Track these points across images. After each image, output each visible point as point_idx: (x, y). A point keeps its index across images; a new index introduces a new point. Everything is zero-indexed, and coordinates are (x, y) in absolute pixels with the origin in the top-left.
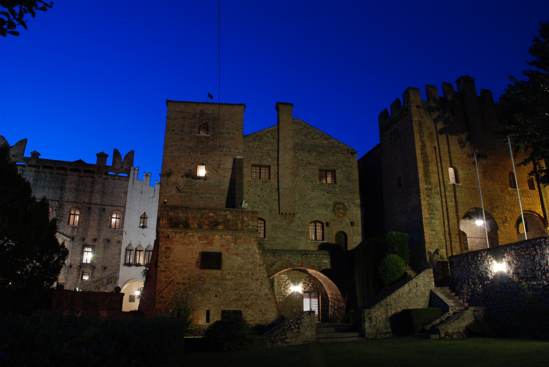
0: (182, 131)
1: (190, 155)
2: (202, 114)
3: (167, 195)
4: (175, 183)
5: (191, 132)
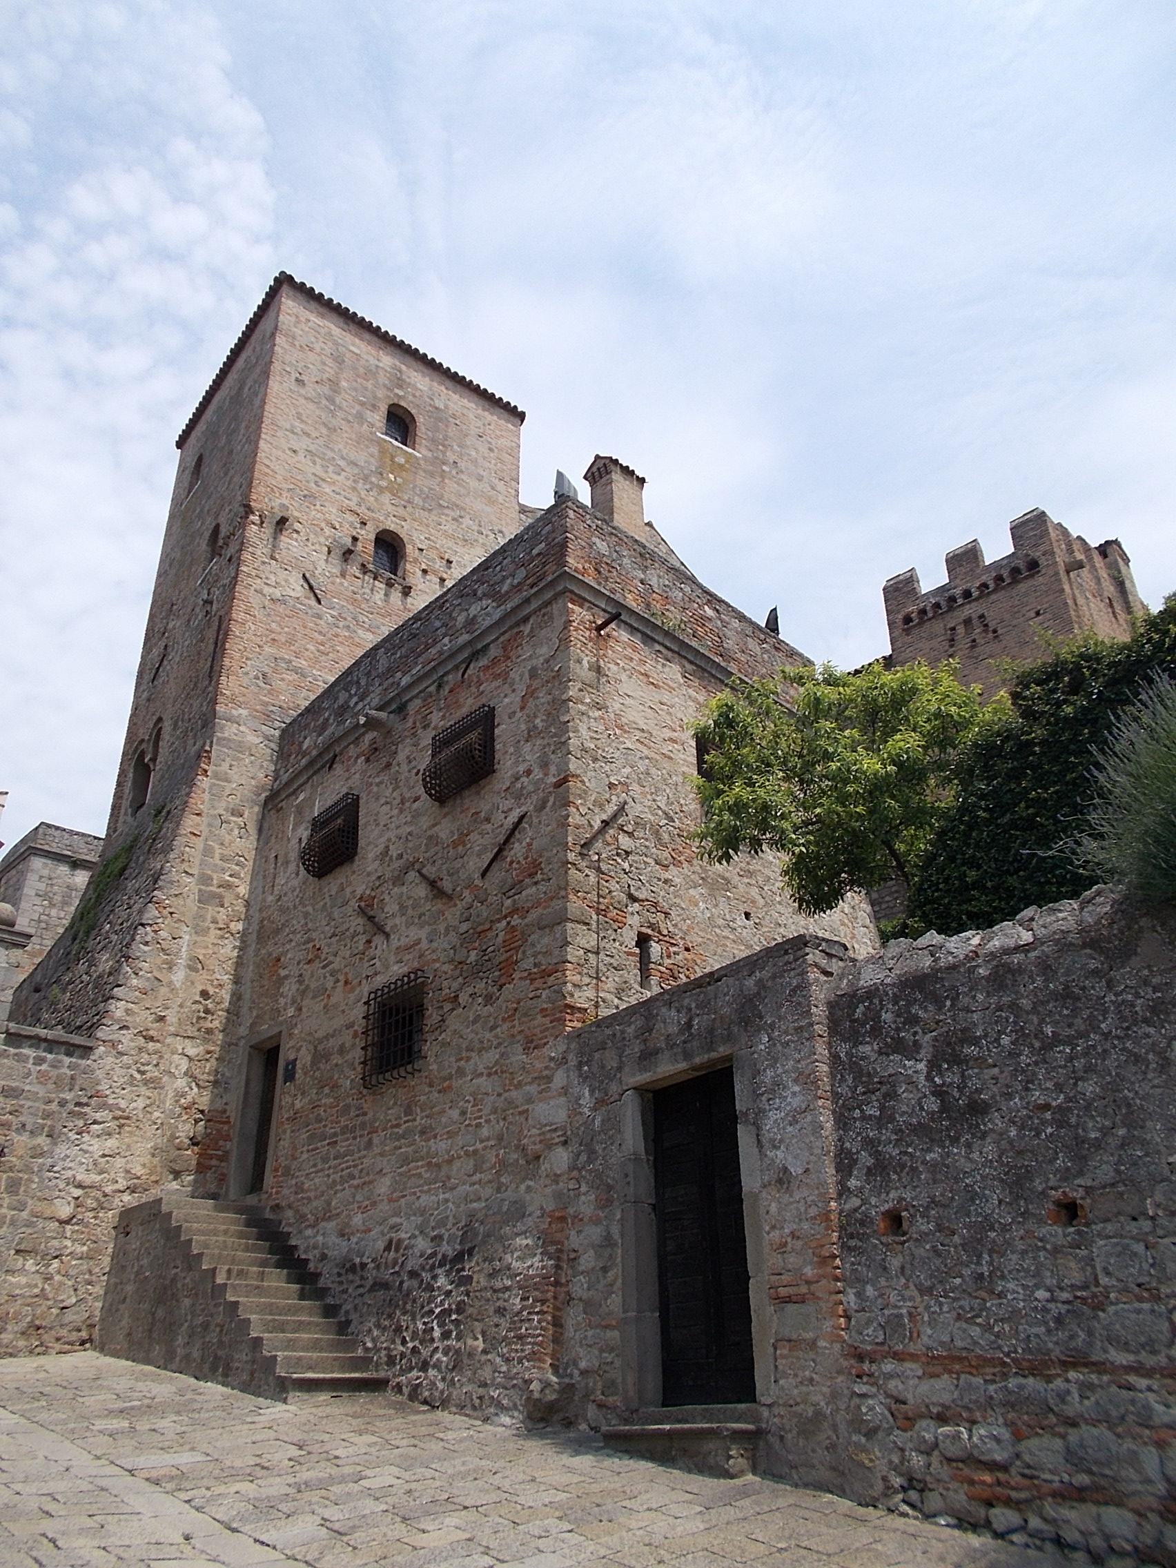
0: (331, 400)
2: (400, 382)
3: (267, 590)
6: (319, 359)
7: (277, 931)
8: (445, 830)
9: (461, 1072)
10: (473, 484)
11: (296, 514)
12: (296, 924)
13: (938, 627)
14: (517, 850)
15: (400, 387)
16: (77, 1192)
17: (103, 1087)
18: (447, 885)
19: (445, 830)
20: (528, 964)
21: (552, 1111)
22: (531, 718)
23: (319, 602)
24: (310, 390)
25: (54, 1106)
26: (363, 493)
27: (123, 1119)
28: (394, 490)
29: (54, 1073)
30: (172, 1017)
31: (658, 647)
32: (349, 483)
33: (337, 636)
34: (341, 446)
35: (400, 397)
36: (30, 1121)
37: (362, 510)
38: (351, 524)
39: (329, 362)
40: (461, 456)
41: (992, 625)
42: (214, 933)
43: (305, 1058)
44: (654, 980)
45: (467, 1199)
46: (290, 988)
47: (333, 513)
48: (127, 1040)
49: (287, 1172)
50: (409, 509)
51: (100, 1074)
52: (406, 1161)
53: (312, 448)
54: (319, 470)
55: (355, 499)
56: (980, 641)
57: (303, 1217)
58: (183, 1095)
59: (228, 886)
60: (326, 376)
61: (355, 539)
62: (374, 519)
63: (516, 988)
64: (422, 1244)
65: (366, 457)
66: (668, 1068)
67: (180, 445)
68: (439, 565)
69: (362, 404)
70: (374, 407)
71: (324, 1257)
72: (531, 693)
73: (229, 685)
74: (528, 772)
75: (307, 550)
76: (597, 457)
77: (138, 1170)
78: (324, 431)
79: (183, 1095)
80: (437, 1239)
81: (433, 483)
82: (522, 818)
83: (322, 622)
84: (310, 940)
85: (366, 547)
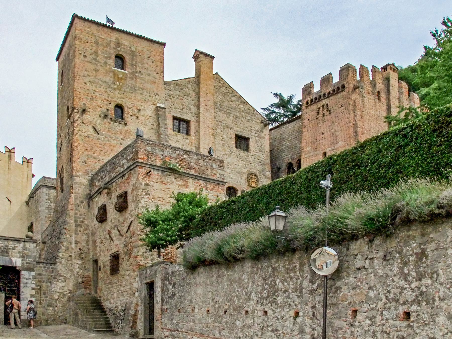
1: (106, 92)
2: (118, 44)
3: (83, 134)
4: (90, 122)
5: (106, 63)
6: (90, 45)
7: (95, 234)
8: (121, 219)
9: (125, 275)
12: (98, 233)
13: (314, 107)
14: (131, 228)
15: (119, 47)
16: (58, 294)
17: (60, 272)
18: (121, 232)
19: (121, 219)
20: (133, 254)
21: (136, 285)
22: (133, 197)
23: (98, 134)
25: (50, 277)
26: (109, 92)
27: (65, 279)
28: (120, 88)
29: (48, 270)
30: (73, 256)
31: (166, 173)
32: (104, 90)
33: (105, 144)
35: (119, 51)
36: (45, 280)
37: (110, 99)
38: (106, 105)
39: (94, 45)
42: (80, 234)
43: (102, 266)
44: (162, 257)
45: (127, 299)
46: (98, 249)
47: (100, 102)
48: (63, 261)
49: (101, 290)
51: (58, 269)
52: (118, 291)
54: (94, 88)
55: (107, 95)
56: (326, 114)
57: (104, 299)
59: (82, 222)
60: (93, 51)
62: (113, 101)
63: (131, 260)
64: (120, 307)
65: (109, 79)
66: (148, 281)
67: (57, 59)
69: (106, 58)
70: (110, 58)
71: (107, 308)
72: (133, 191)
74: (133, 210)
77: (70, 289)
80: (122, 306)
81: (132, 82)
82: (132, 221)
83: (100, 141)
84: (100, 238)
85: (112, 113)
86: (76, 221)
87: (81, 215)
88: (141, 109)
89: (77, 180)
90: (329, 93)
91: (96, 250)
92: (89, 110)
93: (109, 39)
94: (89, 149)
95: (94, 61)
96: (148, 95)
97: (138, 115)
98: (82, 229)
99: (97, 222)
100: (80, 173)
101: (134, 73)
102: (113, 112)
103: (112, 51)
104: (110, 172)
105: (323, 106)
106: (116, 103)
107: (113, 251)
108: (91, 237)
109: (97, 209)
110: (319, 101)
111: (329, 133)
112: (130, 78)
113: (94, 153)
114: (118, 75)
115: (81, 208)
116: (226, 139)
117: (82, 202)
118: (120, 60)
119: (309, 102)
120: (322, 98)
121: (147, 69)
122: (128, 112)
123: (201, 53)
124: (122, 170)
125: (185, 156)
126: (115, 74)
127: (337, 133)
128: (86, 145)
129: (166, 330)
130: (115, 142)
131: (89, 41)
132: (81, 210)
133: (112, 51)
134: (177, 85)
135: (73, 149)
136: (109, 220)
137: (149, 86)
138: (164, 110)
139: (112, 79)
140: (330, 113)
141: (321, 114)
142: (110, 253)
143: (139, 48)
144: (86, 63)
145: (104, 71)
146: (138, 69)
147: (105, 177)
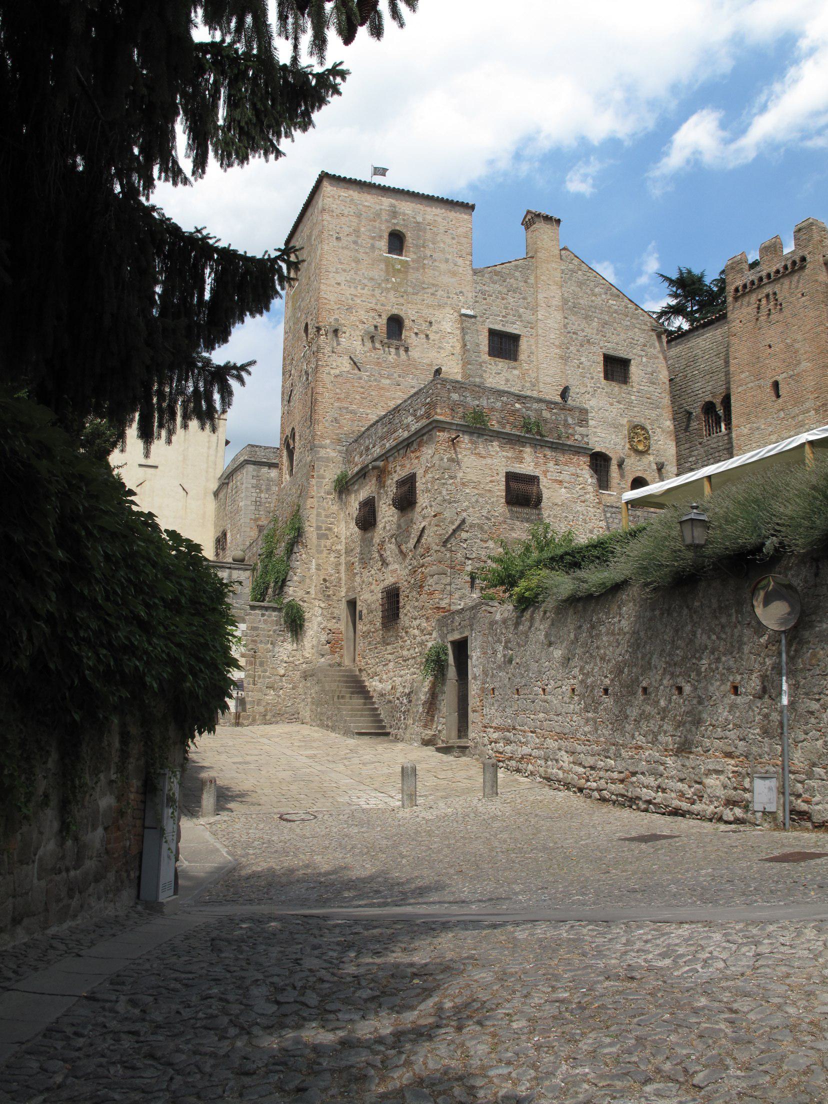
0: (355, 242)
1: (373, 296)
2: (394, 214)
3: (332, 372)
5: (373, 247)
10: (443, 266)
11: (343, 322)
15: (395, 217)
24: (345, 241)
29: (270, 619)
30: (312, 591)
34: (364, 271)
37: (378, 307)
38: (373, 318)
40: (434, 250)
41: (780, 300)
47: (363, 315)
50: (405, 297)
53: (348, 278)
58: (322, 623)
61: (376, 327)
65: (378, 272)
68: (424, 326)
69: (373, 238)
70: (381, 237)
73: (319, 429)
75: (352, 341)
76: (528, 212)
78: (353, 265)
79: (322, 623)
86: (319, 528)
87: (327, 516)
88: (433, 321)
89: (322, 453)
90: (778, 272)
91: (353, 581)
92: (344, 329)
93: (378, 207)
94: (342, 396)
95: (353, 246)
96: (445, 295)
97: (428, 332)
98: (328, 543)
99: (357, 529)
100: (328, 441)
101: (419, 260)
102: (385, 329)
103: (383, 227)
104: (382, 438)
105: (767, 296)
106: (390, 314)
107: (387, 583)
108: (343, 557)
109: (356, 505)
110: (759, 287)
111: (782, 346)
112: (413, 268)
113: (351, 403)
114: (393, 266)
115: (328, 503)
116: (587, 364)
117: (329, 493)
118: (397, 241)
119: (740, 288)
120: (765, 281)
121: (443, 251)
122: (411, 329)
123: (539, 215)
124: (406, 434)
125: (518, 406)
126: (387, 261)
127: (797, 346)
128: (338, 390)
129: (492, 730)
130: (388, 381)
131: (346, 212)
132: (327, 507)
133: (383, 227)
134: (497, 273)
135: (316, 399)
136: (380, 525)
137: (446, 279)
138: (473, 320)
139: (382, 273)
140: (781, 309)
141: (764, 311)
142: (382, 586)
143: (429, 218)
144: (340, 250)
145: (370, 262)
146: (428, 253)
147: (374, 447)
